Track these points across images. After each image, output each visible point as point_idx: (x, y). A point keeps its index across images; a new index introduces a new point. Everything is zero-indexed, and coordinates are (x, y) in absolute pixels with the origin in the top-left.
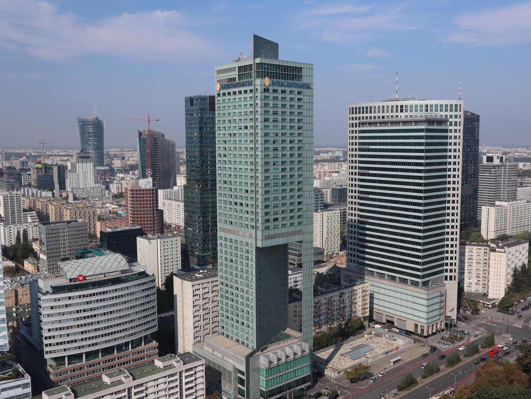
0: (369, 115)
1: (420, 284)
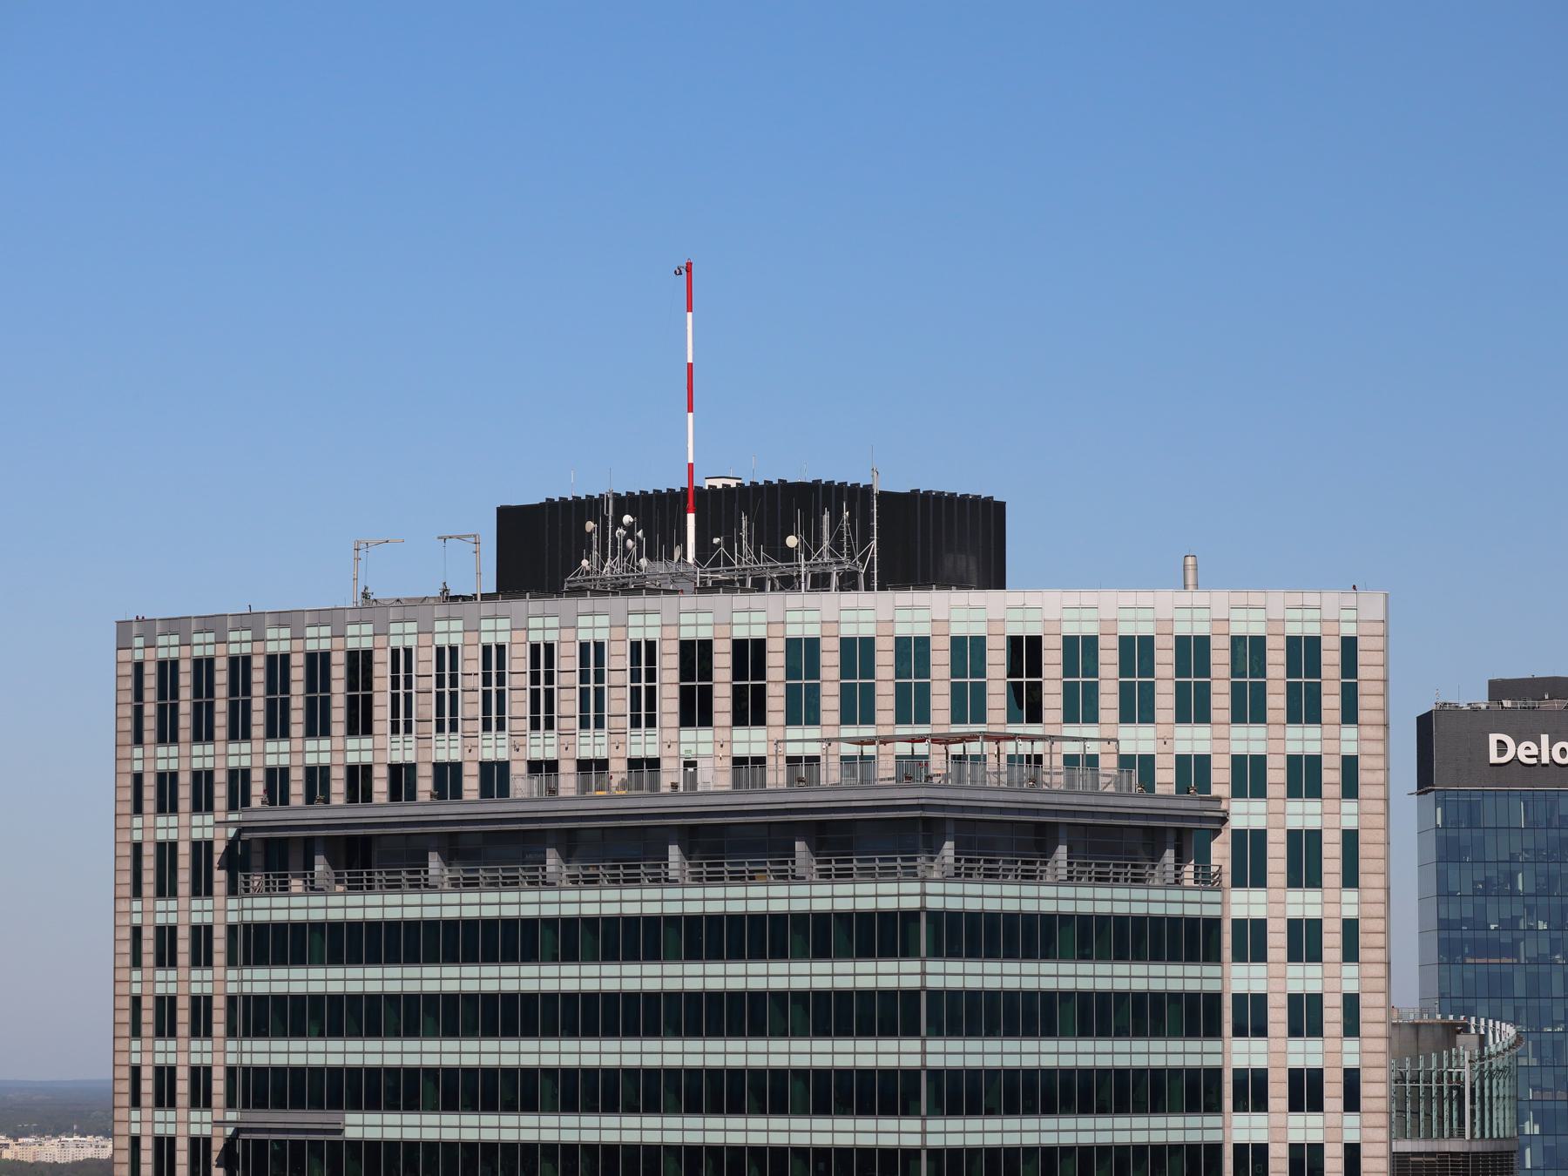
0: (338, 751)
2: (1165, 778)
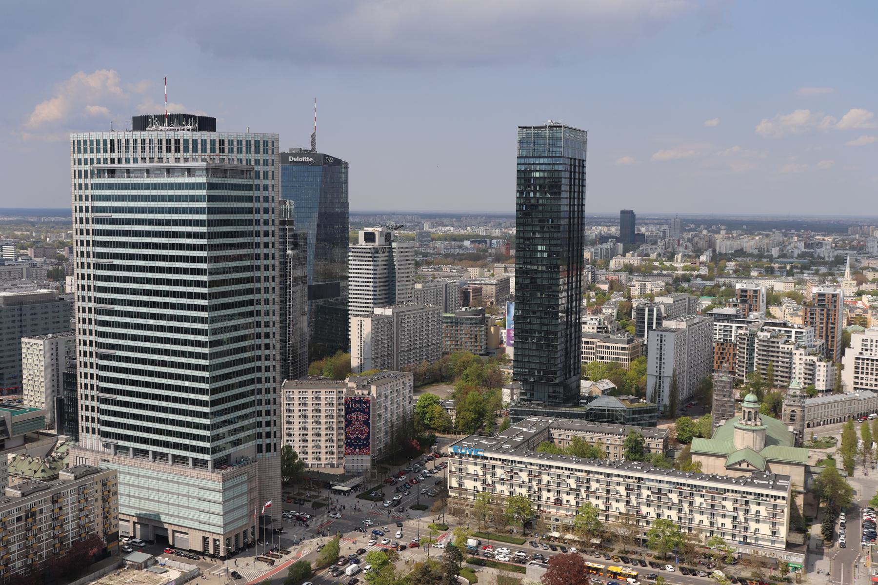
1: (210, 463)
2: (244, 162)
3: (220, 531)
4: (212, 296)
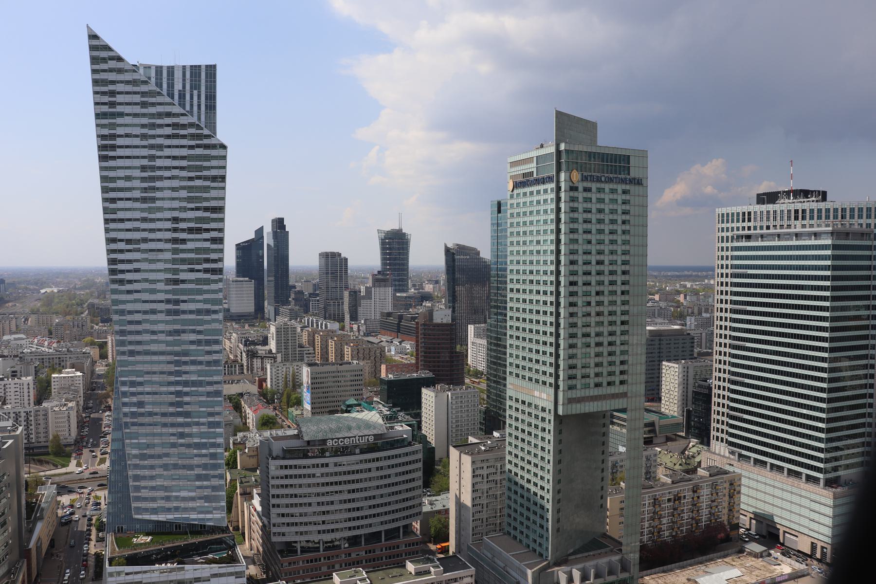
0: (746, 224)
1: (822, 482)
3: (829, 541)
4: (832, 340)
